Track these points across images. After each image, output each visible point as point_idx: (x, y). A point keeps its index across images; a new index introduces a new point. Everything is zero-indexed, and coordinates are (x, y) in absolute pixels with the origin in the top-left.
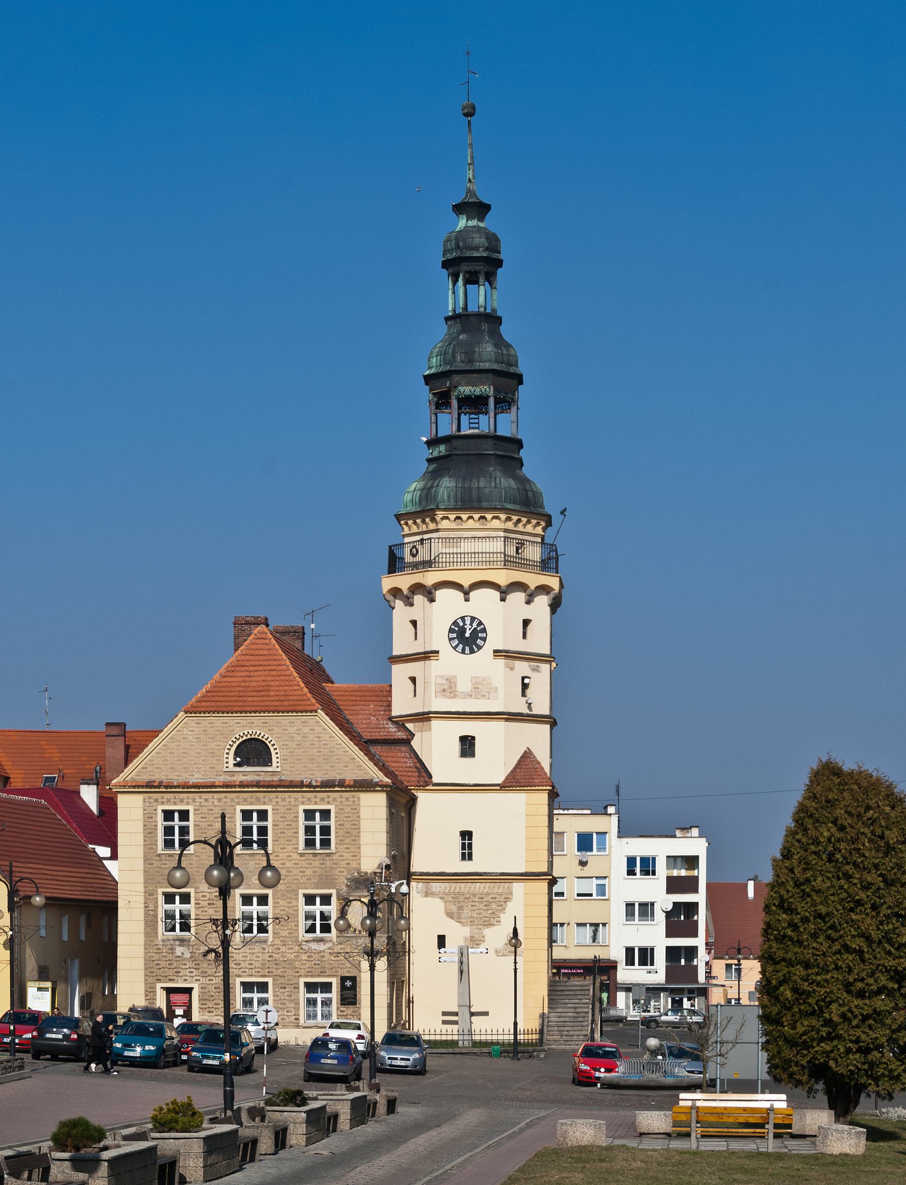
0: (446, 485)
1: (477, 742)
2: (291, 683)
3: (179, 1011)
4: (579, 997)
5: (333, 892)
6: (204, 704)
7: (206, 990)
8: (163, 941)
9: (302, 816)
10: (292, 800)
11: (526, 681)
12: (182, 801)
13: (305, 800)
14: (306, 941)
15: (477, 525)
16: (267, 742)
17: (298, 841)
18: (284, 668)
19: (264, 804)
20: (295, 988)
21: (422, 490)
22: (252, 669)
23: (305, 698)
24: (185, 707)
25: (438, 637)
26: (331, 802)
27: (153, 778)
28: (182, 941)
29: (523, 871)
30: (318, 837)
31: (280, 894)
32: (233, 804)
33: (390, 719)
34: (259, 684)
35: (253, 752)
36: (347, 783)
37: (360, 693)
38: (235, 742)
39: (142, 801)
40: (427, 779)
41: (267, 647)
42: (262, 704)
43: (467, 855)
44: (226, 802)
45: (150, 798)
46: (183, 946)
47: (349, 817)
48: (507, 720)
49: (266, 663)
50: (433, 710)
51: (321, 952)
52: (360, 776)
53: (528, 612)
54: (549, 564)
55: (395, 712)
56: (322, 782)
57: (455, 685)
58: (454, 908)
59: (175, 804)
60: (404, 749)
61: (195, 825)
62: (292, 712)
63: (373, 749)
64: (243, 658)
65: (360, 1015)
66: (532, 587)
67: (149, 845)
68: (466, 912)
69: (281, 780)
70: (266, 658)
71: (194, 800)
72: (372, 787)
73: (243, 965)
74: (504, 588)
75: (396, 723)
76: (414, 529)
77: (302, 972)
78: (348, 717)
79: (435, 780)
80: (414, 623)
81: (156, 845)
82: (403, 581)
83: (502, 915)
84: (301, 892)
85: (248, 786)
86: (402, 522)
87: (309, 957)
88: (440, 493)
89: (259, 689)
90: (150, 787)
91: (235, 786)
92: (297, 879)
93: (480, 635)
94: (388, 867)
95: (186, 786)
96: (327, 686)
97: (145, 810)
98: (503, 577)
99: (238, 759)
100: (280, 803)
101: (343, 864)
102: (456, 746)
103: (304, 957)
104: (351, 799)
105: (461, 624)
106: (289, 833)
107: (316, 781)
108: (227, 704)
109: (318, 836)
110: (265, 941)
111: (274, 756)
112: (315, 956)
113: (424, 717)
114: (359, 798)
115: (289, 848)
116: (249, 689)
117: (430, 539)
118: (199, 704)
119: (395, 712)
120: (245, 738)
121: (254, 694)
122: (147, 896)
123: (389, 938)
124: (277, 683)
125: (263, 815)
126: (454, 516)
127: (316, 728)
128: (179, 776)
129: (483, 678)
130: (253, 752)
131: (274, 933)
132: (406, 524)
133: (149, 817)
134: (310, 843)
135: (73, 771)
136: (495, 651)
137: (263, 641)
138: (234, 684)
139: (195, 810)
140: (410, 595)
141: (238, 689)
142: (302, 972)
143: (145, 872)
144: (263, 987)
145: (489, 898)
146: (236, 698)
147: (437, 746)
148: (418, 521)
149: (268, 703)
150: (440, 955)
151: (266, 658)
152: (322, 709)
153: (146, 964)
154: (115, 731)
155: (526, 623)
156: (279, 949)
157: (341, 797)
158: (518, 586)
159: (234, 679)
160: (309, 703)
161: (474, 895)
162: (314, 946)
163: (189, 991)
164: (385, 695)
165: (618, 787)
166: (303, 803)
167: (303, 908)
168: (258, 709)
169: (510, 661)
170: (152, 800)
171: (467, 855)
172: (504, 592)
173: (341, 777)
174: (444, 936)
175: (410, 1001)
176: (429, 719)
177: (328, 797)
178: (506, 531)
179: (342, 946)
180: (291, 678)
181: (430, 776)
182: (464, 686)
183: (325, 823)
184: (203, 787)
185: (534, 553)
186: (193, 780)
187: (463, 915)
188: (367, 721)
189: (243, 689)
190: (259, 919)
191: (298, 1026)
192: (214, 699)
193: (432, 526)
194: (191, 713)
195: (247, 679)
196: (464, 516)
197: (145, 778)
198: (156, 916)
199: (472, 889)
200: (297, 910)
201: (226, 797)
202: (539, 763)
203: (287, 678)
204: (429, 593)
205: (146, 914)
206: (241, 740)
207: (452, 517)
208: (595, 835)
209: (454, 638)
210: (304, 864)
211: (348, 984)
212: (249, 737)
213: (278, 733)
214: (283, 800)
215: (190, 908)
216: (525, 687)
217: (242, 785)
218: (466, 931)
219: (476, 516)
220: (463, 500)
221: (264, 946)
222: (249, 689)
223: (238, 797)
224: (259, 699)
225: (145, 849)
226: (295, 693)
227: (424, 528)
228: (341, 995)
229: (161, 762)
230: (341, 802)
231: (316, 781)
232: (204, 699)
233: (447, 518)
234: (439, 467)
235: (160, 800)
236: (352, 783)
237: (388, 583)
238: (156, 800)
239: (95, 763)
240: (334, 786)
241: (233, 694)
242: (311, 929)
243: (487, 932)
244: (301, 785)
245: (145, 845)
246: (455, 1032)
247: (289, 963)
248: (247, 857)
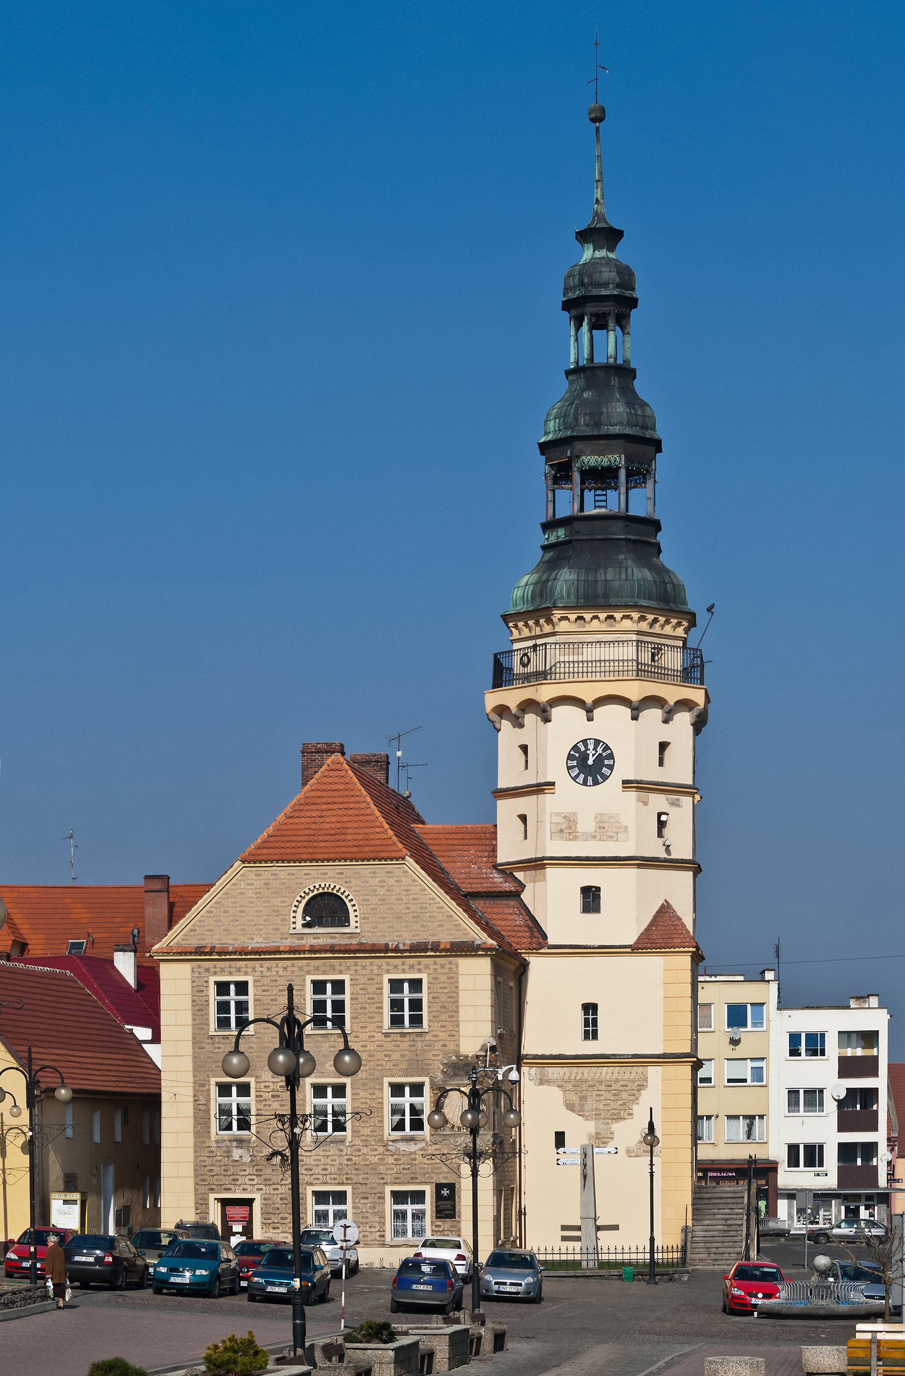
0: (566, 578)
1: (602, 893)
2: (372, 824)
3: (237, 1228)
4: (730, 1206)
5: (426, 1080)
6: (265, 851)
7: (270, 1202)
8: (217, 1142)
9: (386, 987)
10: (375, 968)
11: (663, 818)
12: (239, 970)
13: (391, 967)
14: (393, 1141)
15: (604, 627)
16: (343, 897)
17: (382, 1017)
18: (363, 805)
19: (341, 972)
20: (379, 1198)
21: (536, 584)
22: (324, 807)
23: (390, 842)
24: (243, 855)
25: (555, 767)
26: (422, 970)
27: (203, 943)
28: (240, 1142)
29: (660, 1052)
30: (407, 1013)
31: (360, 1083)
32: (302, 973)
33: (495, 867)
34: (333, 825)
35: (326, 909)
36: (442, 946)
37: (457, 836)
38: (304, 898)
39: (190, 971)
40: (541, 940)
41: (342, 780)
42: (337, 850)
43: (591, 1033)
44: (293, 972)
45: (199, 967)
46: (241, 1148)
47: (445, 988)
48: (639, 866)
49: (341, 800)
50: (548, 855)
51: (411, 1153)
52: (459, 937)
53: (665, 733)
54: (692, 673)
55: (501, 858)
56: (412, 945)
57: (576, 823)
58: (575, 1099)
59: (231, 974)
60: (512, 903)
61: (255, 1000)
62: (374, 860)
63: (475, 904)
64: (313, 794)
65: (459, 1230)
66: (671, 702)
67: (199, 1025)
68: (591, 1104)
69: (360, 944)
70: (341, 793)
71: (254, 969)
72: (473, 950)
73: (316, 1170)
74: (635, 704)
75: (502, 872)
76: (526, 633)
77: (388, 1179)
78: (443, 865)
79: (551, 941)
80: (524, 748)
81: (208, 1025)
82: (511, 697)
83: (634, 1107)
84: (387, 1080)
85: (320, 951)
86: (511, 624)
87: (396, 1160)
88: (558, 588)
89: (333, 832)
90: (199, 953)
91: (304, 952)
92: (382, 1065)
93: (606, 762)
94: (493, 1049)
95: (244, 952)
96: (417, 827)
97: (193, 982)
98: (635, 691)
99: (308, 919)
100: (360, 972)
101: (438, 1045)
102: (577, 899)
103: (391, 1160)
104: (447, 966)
105: (583, 749)
106: (372, 1008)
107: (404, 944)
108: (294, 851)
109: (407, 1012)
110: (343, 1141)
111: (352, 915)
112: (404, 1159)
113: (537, 864)
114: (457, 965)
115: (372, 1027)
116: (321, 832)
117: (545, 644)
118: (260, 852)
119: (501, 858)
120: (316, 892)
121: (327, 838)
122: (197, 1087)
123: (494, 1136)
124: (356, 825)
125: (339, 987)
126: (575, 616)
127: (403, 879)
128: (236, 939)
129: (611, 814)
130: (326, 909)
131: (353, 1131)
132: (516, 626)
133: (198, 991)
134: (397, 1021)
135: (105, 935)
136: (624, 782)
137: (337, 773)
138: (302, 827)
139: (255, 981)
140: (519, 714)
141: (307, 832)
142: (388, 1179)
143: (194, 1057)
144: (340, 1197)
146: (306, 844)
147: (553, 901)
148: (531, 623)
149: (343, 849)
150: (558, 1156)
151: (341, 793)
152: (411, 856)
153: (196, 1170)
154: (157, 885)
155: (663, 746)
156: (360, 1150)
157: (435, 963)
158: (654, 701)
159: (302, 820)
160: (395, 848)
161: (600, 1082)
162: (403, 1146)
163: (249, 1202)
164: (488, 838)
165: (778, 947)
166: (388, 972)
167: (389, 1100)
168: (332, 856)
169: (643, 794)
170: (202, 970)
171: (591, 1033)
172: (636, 709)
173: (434, 939)
174: (563, 1133)
175: (521, 1213)
176: (543, 867)
177: (419, 963)
178: (639, 633)
179: (437, 1146)
180: (372, 818)
181: (545, 937)
182: (586, 825)
183: (416, 996)
184: (265, 953)
185: (673, 660)
186: (252, 945)
187: (586, 1107)
188: (467, 870)
189: (313, 832)
190: (335, 1114)
191: (383, 1245)
192: (276, 845)
193: (547, 629)
194: (249, 863)
195: (318, 820)
196: (588, 616)
197: (194, 942)
198: (208, 1111)
199: (598, 1075)
200: (382, 1103)
201: (293, 965)
202: (679, 919)
203: (367, 818)
204: (543, 712)
205: (196, 1110)
206: (311, 895)
207: (573, 617)
208: (749, 1006)
209: (574, 767)
210: (390, 1046)
211: (445, 1192)
212: (321, 891)
213: (356, 886)
214: (364, 968)
215: (250, 1101)
216: (661, 825)
217: (313, 950)
218: (590, 1127)
219: (603, 616)
220: (586, 597)
221: (342, 1147)
222: (321, 832)
223: (308, 965)
224: (333, 844)
225: (193, 1029)
226: (378, 836)
227: (538, 631)
228: (437, 1206)
229: (214, 923)
230: (435, 970)
231: (404, 944)
232: (265, 845)
233: (566, 618)
234: (556, 555)
235: (212, 970)
236: (448, 946)
237: (492, 699)
238: (207, 970)
239: (132, 925)
240: (427, 950)
241: (300, 838)
242: (400, 1126)
243: (616, 1127)
244: (386, 949)
245: (194, 1025)
246: (578, 1250)
247: (373, 1167)
248: (320, 1039)
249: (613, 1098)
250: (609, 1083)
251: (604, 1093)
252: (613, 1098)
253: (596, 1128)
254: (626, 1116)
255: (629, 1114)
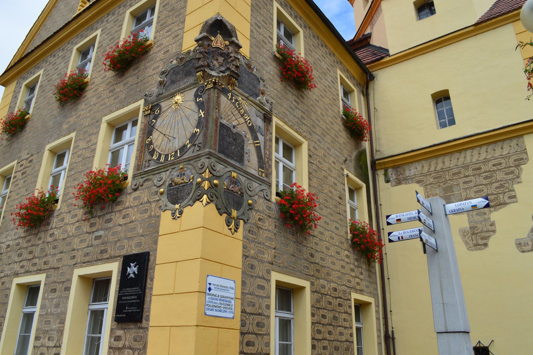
43: (447, 119)
83: (516, 187)
145: (489, 166)
161: (466, 167)
171: (447, 119)
249: (485, 182)
250: (477, 166)
251: (472, 178)
252: (485, 182)
253: (470, 222)
254: (508, 201)
255: (510, 198)
